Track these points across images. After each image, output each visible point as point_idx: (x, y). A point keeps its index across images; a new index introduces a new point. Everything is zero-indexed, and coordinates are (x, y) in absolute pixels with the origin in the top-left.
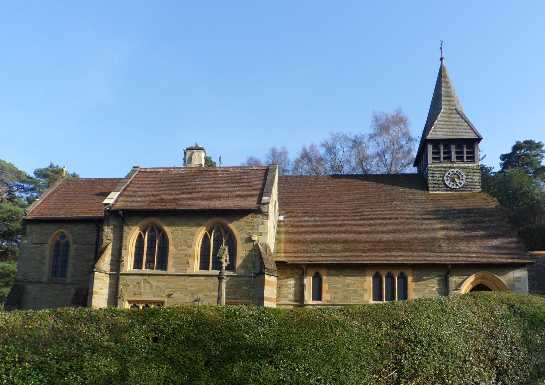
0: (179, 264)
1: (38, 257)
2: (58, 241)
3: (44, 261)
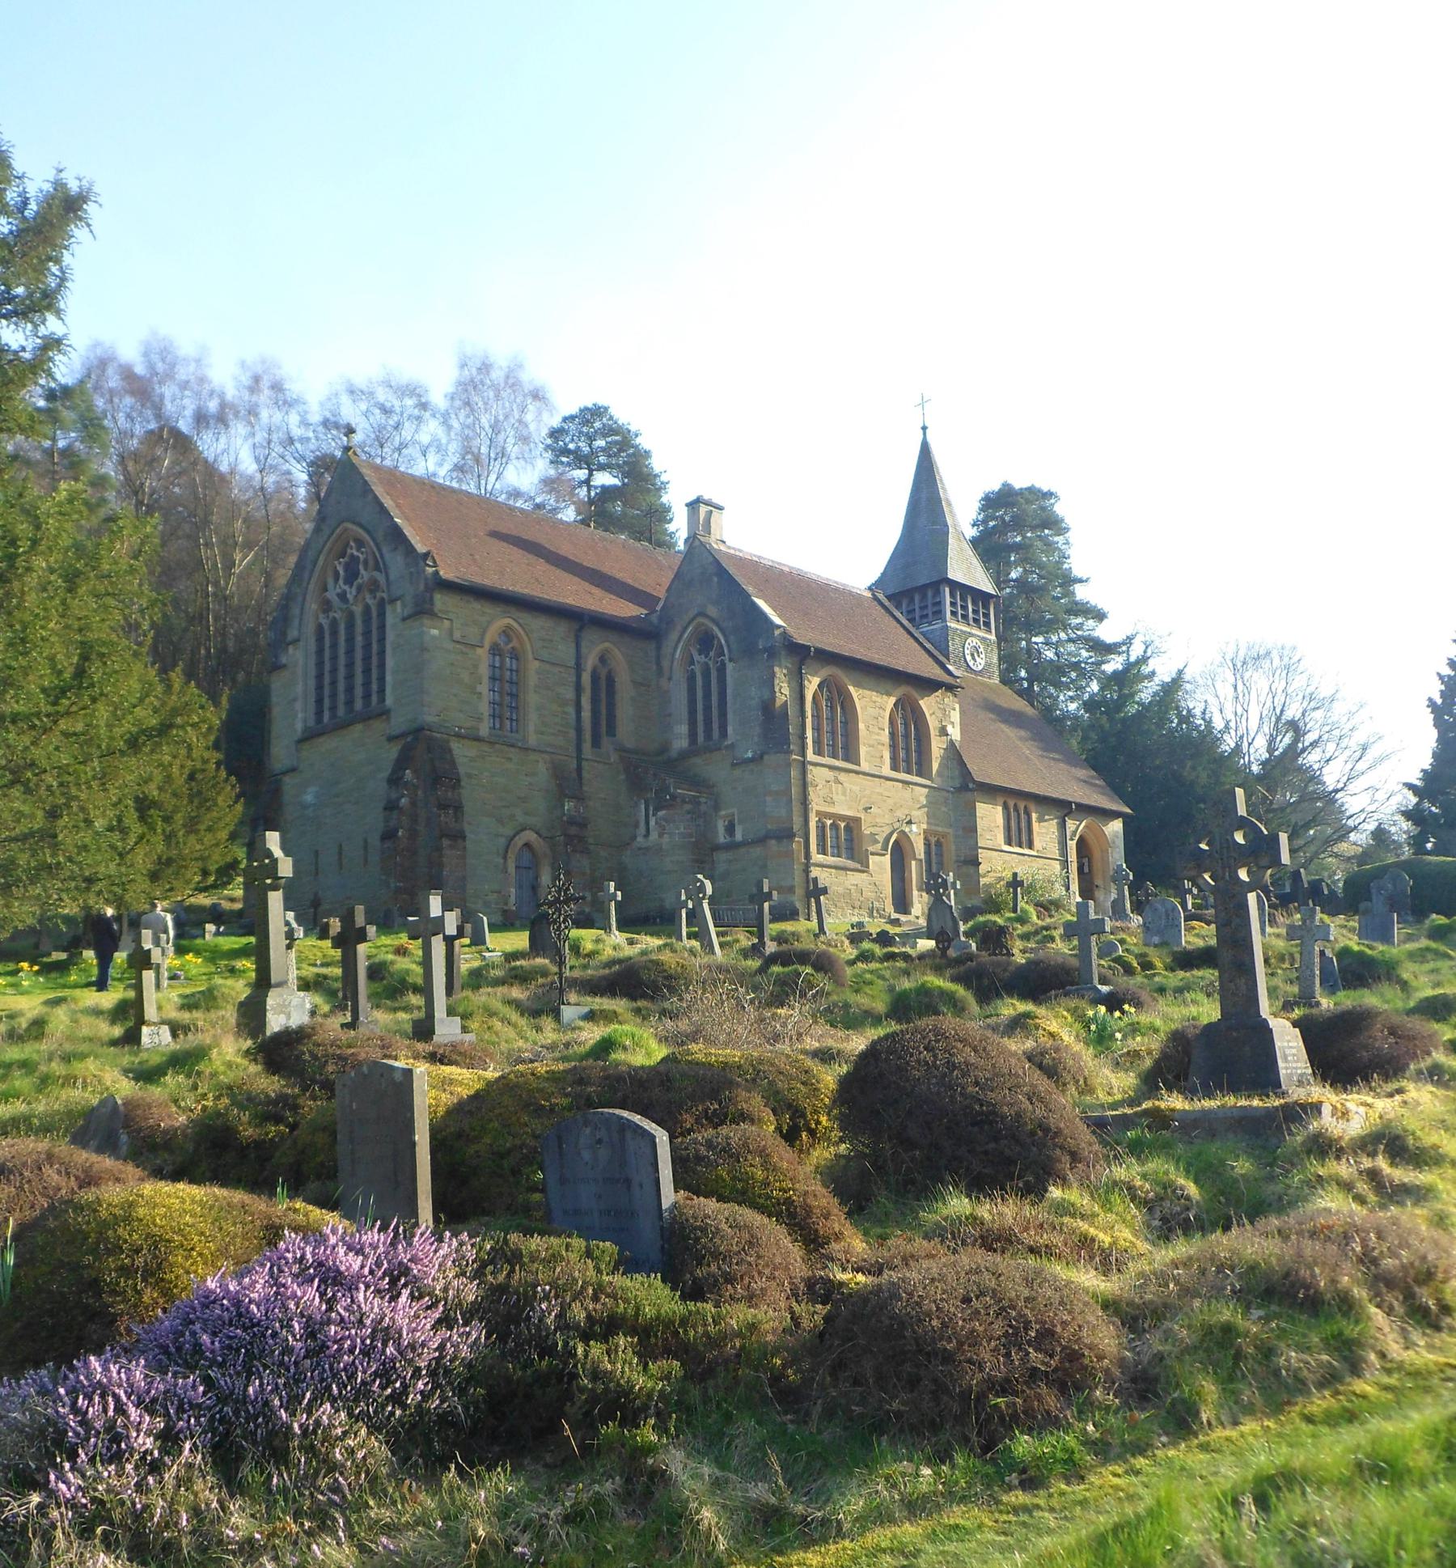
1: (465, 676)
3: (479, 688)
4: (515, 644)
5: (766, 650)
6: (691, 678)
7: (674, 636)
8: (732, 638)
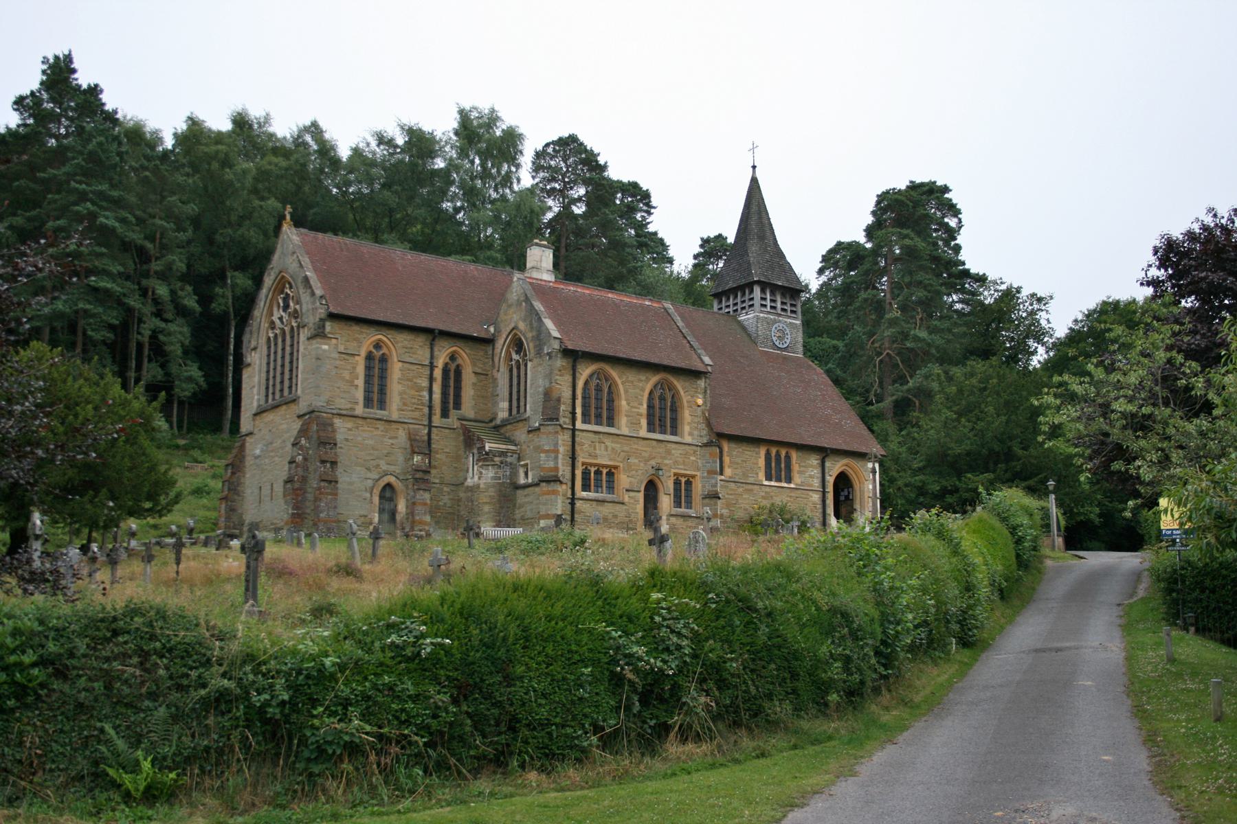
1: (346, 375)
2: (371, 352)
3: (356, 382)
4: (384, 350)
5: (549, 354)
6: (511, 371)
7: (501, 341)
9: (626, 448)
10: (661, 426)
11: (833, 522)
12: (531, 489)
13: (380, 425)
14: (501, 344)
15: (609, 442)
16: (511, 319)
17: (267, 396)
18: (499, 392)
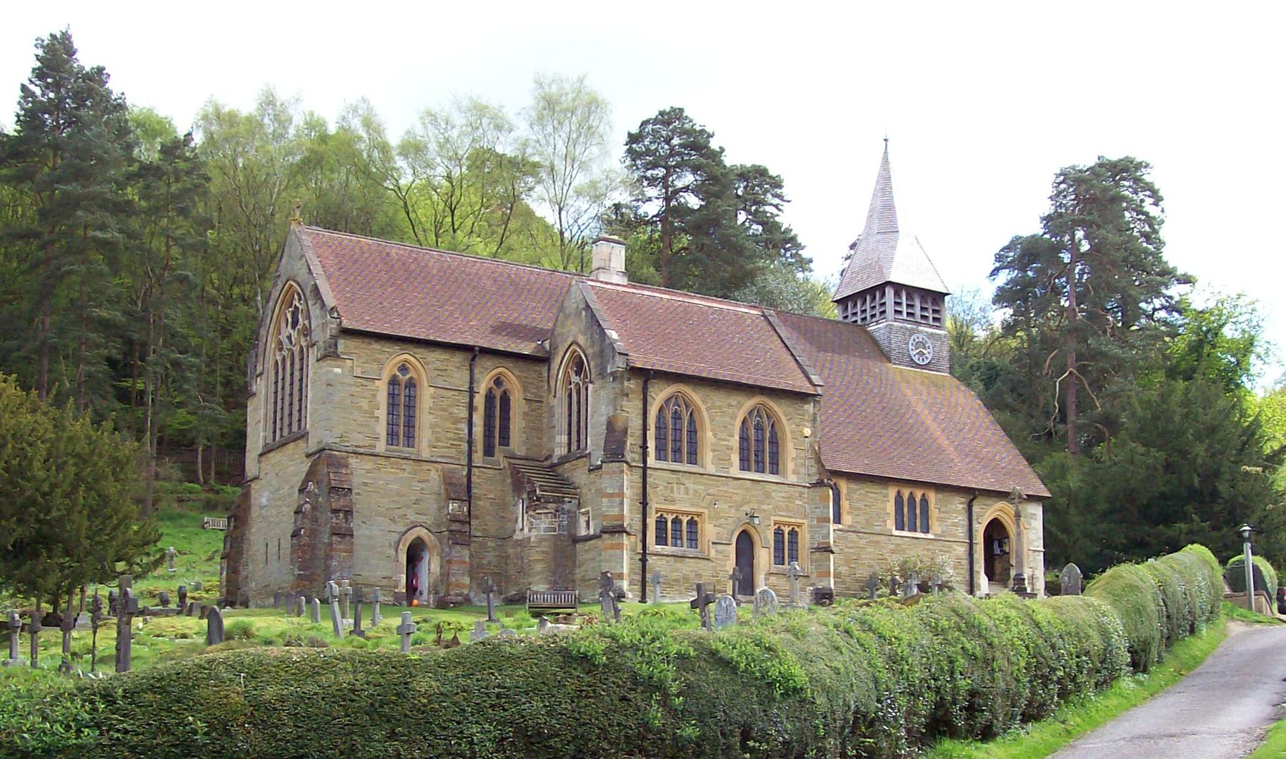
0: (720, 460)
1: (365, 404)
3: (377, 413)
4: (412, 374)
5: (612, 374)
6: (570, 396)
8: (592, 364)
9: (712, 491)
10: (757, 462)
11: (983, 580)
12: (593, 542)
13: (408, 465)
14: (560, 365)
15: (690, 483)
16: (569, 331)
17: (275, 432)
18: (555, 423)
